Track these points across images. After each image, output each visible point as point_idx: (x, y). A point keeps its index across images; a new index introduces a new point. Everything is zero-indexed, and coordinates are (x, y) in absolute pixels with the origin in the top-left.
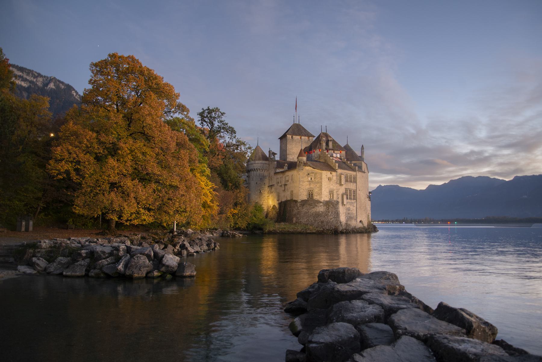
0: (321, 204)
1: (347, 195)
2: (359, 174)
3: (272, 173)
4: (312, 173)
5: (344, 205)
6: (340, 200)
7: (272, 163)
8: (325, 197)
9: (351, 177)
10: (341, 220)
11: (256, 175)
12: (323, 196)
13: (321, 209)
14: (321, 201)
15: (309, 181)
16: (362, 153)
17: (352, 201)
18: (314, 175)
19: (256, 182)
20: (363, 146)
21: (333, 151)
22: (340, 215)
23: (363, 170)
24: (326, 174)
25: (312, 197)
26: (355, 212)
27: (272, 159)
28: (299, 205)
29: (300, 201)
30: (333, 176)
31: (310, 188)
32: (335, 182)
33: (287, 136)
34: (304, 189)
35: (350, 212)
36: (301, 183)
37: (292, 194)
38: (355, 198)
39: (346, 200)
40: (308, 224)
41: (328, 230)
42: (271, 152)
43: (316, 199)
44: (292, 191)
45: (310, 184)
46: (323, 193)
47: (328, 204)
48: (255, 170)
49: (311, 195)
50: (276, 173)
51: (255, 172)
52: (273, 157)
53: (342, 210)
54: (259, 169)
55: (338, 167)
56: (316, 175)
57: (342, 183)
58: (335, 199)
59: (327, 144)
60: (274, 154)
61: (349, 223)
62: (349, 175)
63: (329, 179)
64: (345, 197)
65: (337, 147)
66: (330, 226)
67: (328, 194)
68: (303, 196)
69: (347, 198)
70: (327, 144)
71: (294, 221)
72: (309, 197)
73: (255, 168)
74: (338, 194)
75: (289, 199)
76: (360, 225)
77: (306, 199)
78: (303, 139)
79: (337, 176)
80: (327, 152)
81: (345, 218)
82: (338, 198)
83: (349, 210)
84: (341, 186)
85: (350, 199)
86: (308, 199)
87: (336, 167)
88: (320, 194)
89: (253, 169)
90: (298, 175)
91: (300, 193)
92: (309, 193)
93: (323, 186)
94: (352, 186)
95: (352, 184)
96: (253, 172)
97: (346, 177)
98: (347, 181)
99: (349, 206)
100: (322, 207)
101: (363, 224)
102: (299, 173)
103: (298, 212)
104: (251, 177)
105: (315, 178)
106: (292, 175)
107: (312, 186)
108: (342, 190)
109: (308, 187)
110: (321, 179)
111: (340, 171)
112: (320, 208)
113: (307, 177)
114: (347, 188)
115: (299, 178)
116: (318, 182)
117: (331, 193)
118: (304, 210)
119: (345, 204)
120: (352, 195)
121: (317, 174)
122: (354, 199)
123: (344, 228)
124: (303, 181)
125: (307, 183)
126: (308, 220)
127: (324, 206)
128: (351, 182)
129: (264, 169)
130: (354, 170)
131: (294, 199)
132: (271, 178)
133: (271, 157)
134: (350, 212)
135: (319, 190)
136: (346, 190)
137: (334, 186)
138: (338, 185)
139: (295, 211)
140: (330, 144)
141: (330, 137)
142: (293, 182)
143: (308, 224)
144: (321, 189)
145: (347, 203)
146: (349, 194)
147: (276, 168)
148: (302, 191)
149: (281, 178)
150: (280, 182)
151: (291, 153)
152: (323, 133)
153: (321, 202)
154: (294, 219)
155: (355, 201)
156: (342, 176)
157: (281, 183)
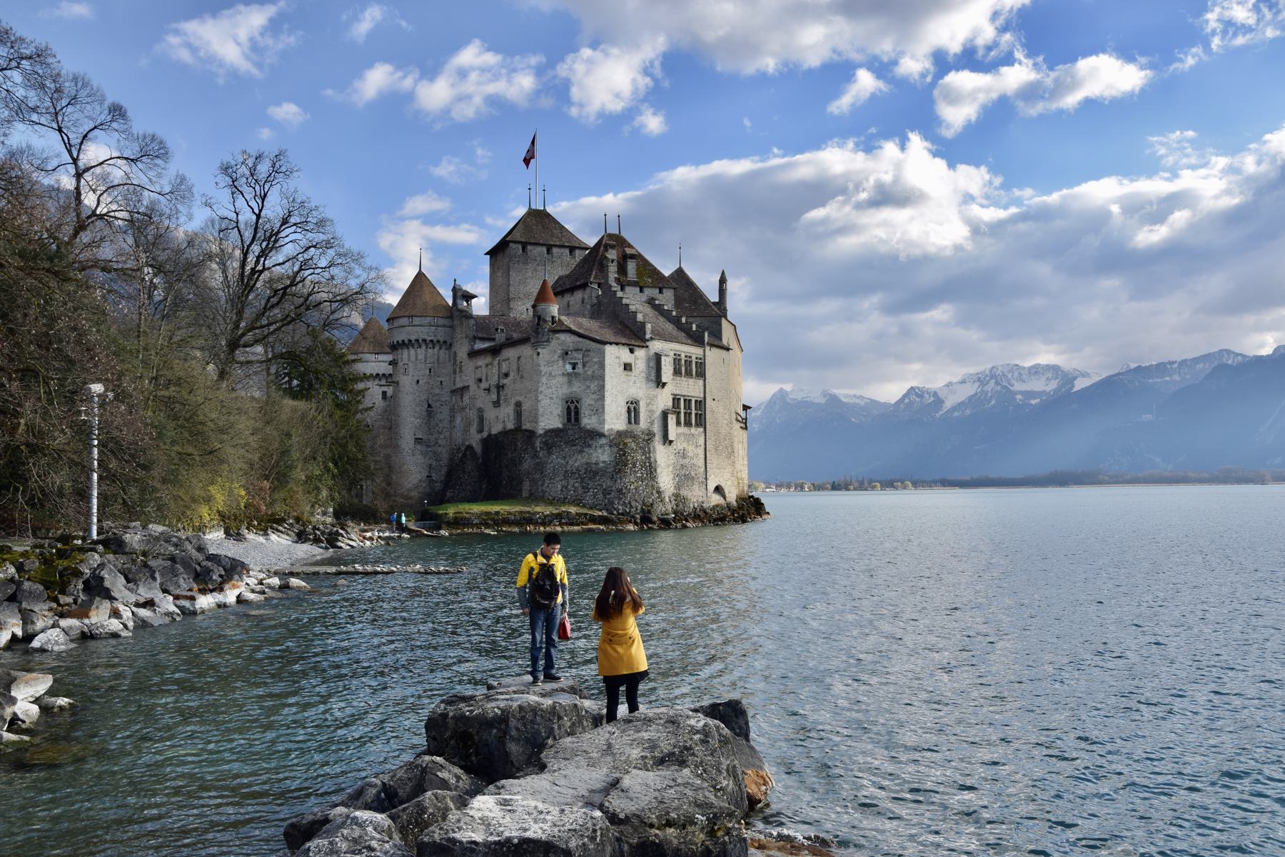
0: (603, 441)
1: (679, 413)
2: (712, 355)
3: (462, 351)
4: (577, 350)
5: (671, 442)
6: (657, 428)
7: (462, 323)
8: (614, 420)
9: (688, 363)
10: (661, 485)
11: (416, 359)
12: (607, 417)
13: (602, 455)
15: (569, 374)
16: (722, 292)
17: (693, 430)
18: (581, 356)
19: (416, 378)
20: (723, 273)
21: (638, 289)
22: (659, 471)
23: (725, 342)
24: (615, 355)
25: (577, 420)
26: (702, 461)
27: (461, 311)
28: (538, 444)
29: (541, 432)
30: (636, 358)
32: (644, 375)
33: (511, 244)
34: (551, 398)
35: (686, 461)
36: (544, 380)
37: (519, 414)
38: (701, 422)
39: (675, 426)
40: (565, 498)
41: (622, 514)
42: (459, 294)
43: (588, 427)
44: (518, 404)
45: (570, 382)
46: (607, 408)
47: (619, 441)
48: (413, 346)
49: (572, 411)
50: (473, 354)
51: (412, 351)
52: (465, 304)
53: (663, 457)
54: (424, 340)
55: (652, 332)
57: (664, 380)
58: (643, 424)
59: (622, 270)
60: (469, 297)
61: (684, 492)
62: (683, 356)
63: (627, 367)
64: (672, 420)
65: (649, 276)
66: (630, 503)
67: (624, 410)
68: (549, 418)
69: (678, 423)
70: (622, 270)
71: (525, 494)
72: (569, 420)
73: (413, 338)
74: (652, 412)
75: (510, 426)
76: (716, 499)
77: (560, 426)
78: (555, 254)
79: (647, 355)
80: (622, 289)
81: (674, 479)
82: (652, 423)
83: (684, 456)
84: (659, 390)
85: (688, 424)
86: (564, 425)
87: (645, 333)
88: (599, 410)
89: (406, 341)
90: (535, 356)
92: (569, 408)
93: (608, 386)
94: (691, 388)
95: (691, 381)
96: (405, 351)
97: (677, 361)
98: (677, 372)
99: (685, 445)
100: (607, 448)
101: (724, 498)
102: (539, 350)
103: (538, 464)
104: (400, 364)
105: (584, 366)
106: (519, 358)
107: (575, 389)
108: (663, 400)
109: (565, 391)
110: (602, 365)
111: (657, 346)
112: (600, 451)
113: (561, 362)
114: (678, 392)
115: (539, 366)
116: (593, 377)
117: (633, 411)
118: (555, 459)
119: (670, 438)
120: (694, 412)
121: (591, 354)
122: (697, 425)
123: (669, 507)
124: (550, 374)
125: (565, 379)
126: (566, 488)
127: (610, 446)
128: (689, 374)
129: (438, 341)
130: (697, 340)
131: (527, 426)
132: (460, 368)
133: (460, 307)
134: (686, 461)
135: (597, 400)
136: (676, 400)
137: (637, 387)
138: (653, 385)
139: (527, 464)
140: (631, 266)
141: (630, 246)
142: (522, 377)
143: (565, 498)
144: (602, 398)
145: (678, 435)
146: (682, 411)
147: (475, 338)
148: (545, 402)
149: (487, 365)
150: (484, 379)
151: (522, 296)
152: (611, 236)
153: (601, 435)
154: (526, 486)
155: (702, 429)
156: (663, 358)
157: (487, 380)
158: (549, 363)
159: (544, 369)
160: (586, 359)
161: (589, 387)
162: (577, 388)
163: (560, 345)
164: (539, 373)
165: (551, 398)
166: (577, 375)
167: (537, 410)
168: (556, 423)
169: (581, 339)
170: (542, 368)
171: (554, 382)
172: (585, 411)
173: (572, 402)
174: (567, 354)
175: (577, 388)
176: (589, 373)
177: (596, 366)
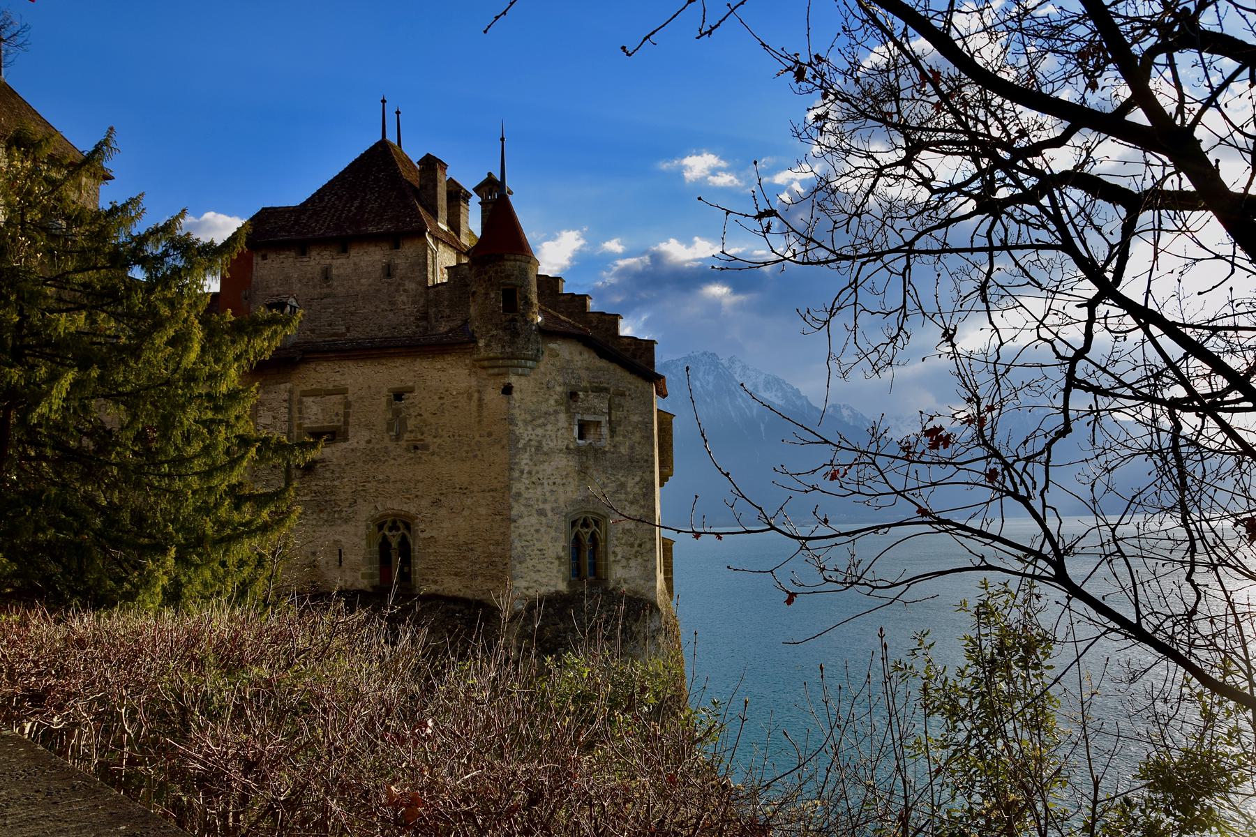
4: (599, 390)
14: (650, 595)
18: (604, 407)
31: (586, 500)
34: (542, 513)
36: (524, 460)
43: (625, 588)
45: (583, 472)
56: (620, 406)
77: (562, 587)
86: (570, 584)
91: (518, 544)
105: (613, 432)
109: (570, 492)
113: (562, 417)
115: (511, 421)
124: (539, 448)
148: (527, 522)
158: (535, 418)
159: (525, 433)
160: (616, 415)
161: (623, 486)
162: (598, 486)
163: (562, 370)
164: (511, 443)
165: (542, 513)
166: (597, 453)
167: (504, 543)
168: (554, 580)
169: (603, 363)
170: (519, 430)
171: (548, 468)
172: (616, 548)
173: (585, 524)
174: (573, 395)
175: (598, 486)
176: (624, 450)
177: (637, 437)
